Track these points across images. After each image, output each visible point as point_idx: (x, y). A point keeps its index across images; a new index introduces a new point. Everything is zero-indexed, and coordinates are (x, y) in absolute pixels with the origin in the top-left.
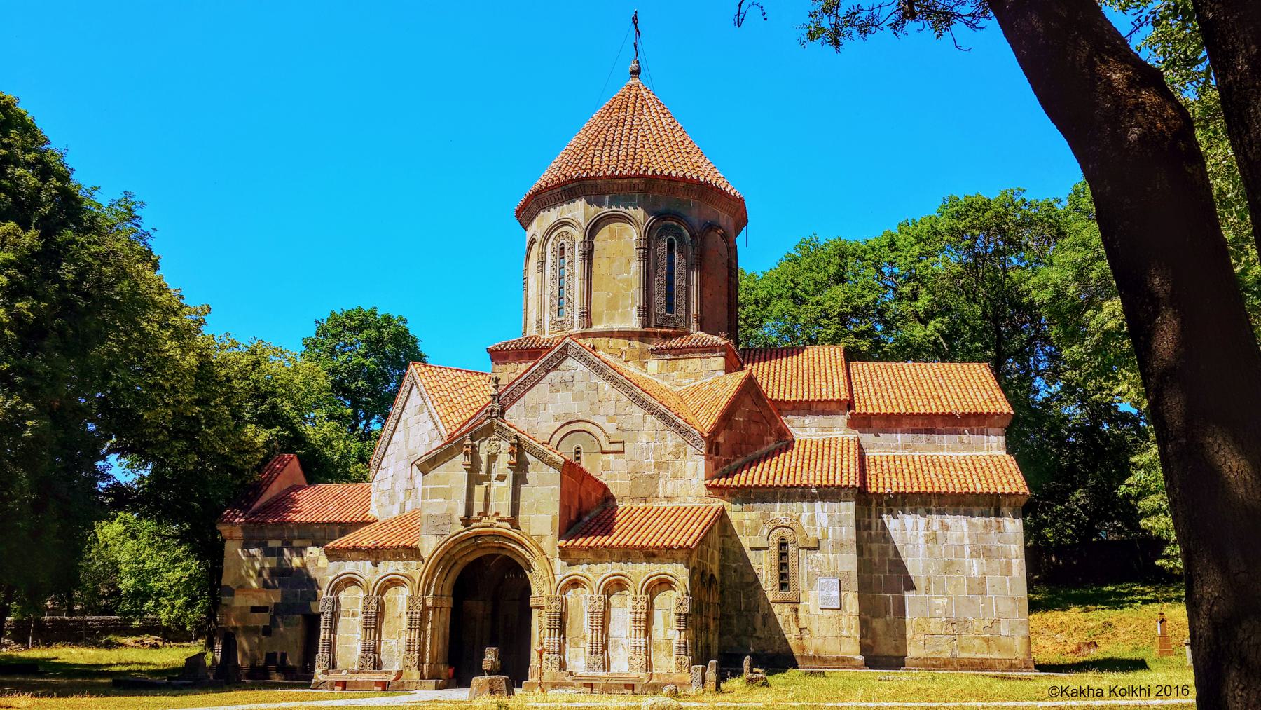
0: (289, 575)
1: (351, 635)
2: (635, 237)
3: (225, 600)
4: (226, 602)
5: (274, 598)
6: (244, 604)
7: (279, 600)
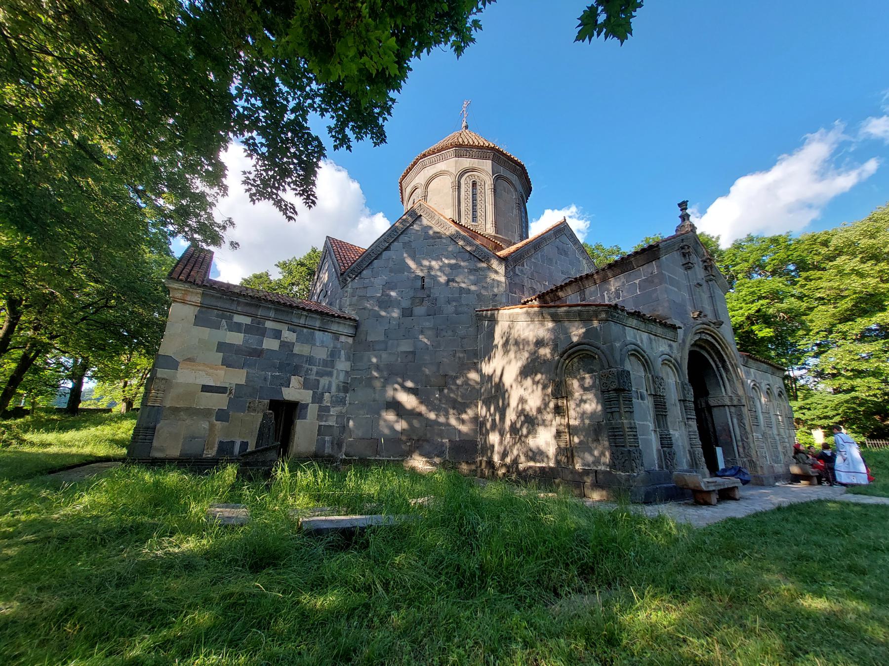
0: (259, 356)
1: (645, 423)
2: (514, 197)
3: (161, 373)
4: (165, 376)
5: (237, 377)
6: (191, 381)
7: (243, 382)
